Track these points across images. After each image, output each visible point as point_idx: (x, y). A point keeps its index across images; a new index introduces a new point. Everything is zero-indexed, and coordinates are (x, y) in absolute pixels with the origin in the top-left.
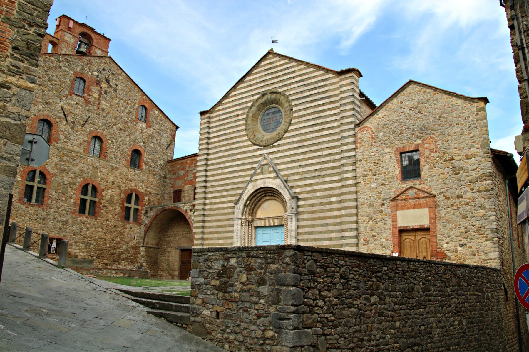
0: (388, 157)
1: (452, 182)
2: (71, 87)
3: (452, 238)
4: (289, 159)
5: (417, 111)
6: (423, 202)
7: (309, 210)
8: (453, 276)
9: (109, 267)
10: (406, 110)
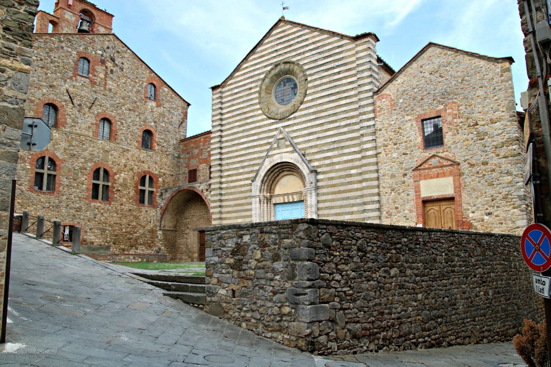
0: (409, 124)
1: (476, 148)
2: (75, 69)
3: (478, 207)
4: (306, 132)
5: (438, 75)
6: (447, 170)
7: (329, 184)
8: (477, 246)
9: (126, 253)
10: (427, 75)
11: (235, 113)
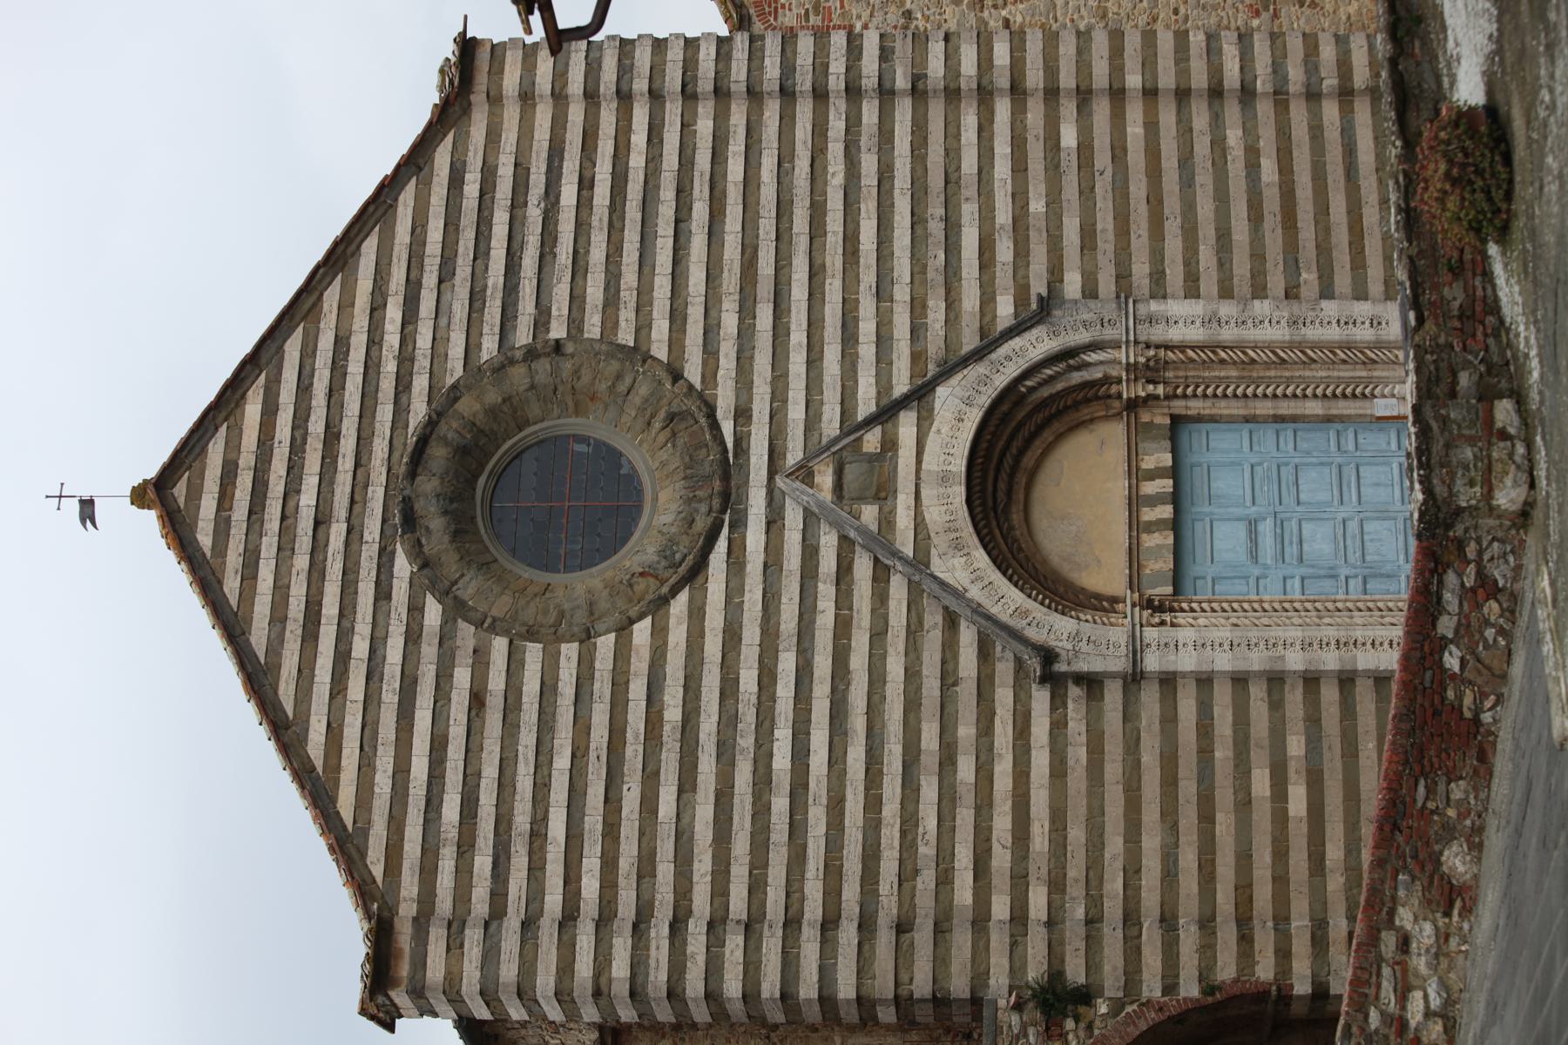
7: (1110, 247)
11: (593, 821)
